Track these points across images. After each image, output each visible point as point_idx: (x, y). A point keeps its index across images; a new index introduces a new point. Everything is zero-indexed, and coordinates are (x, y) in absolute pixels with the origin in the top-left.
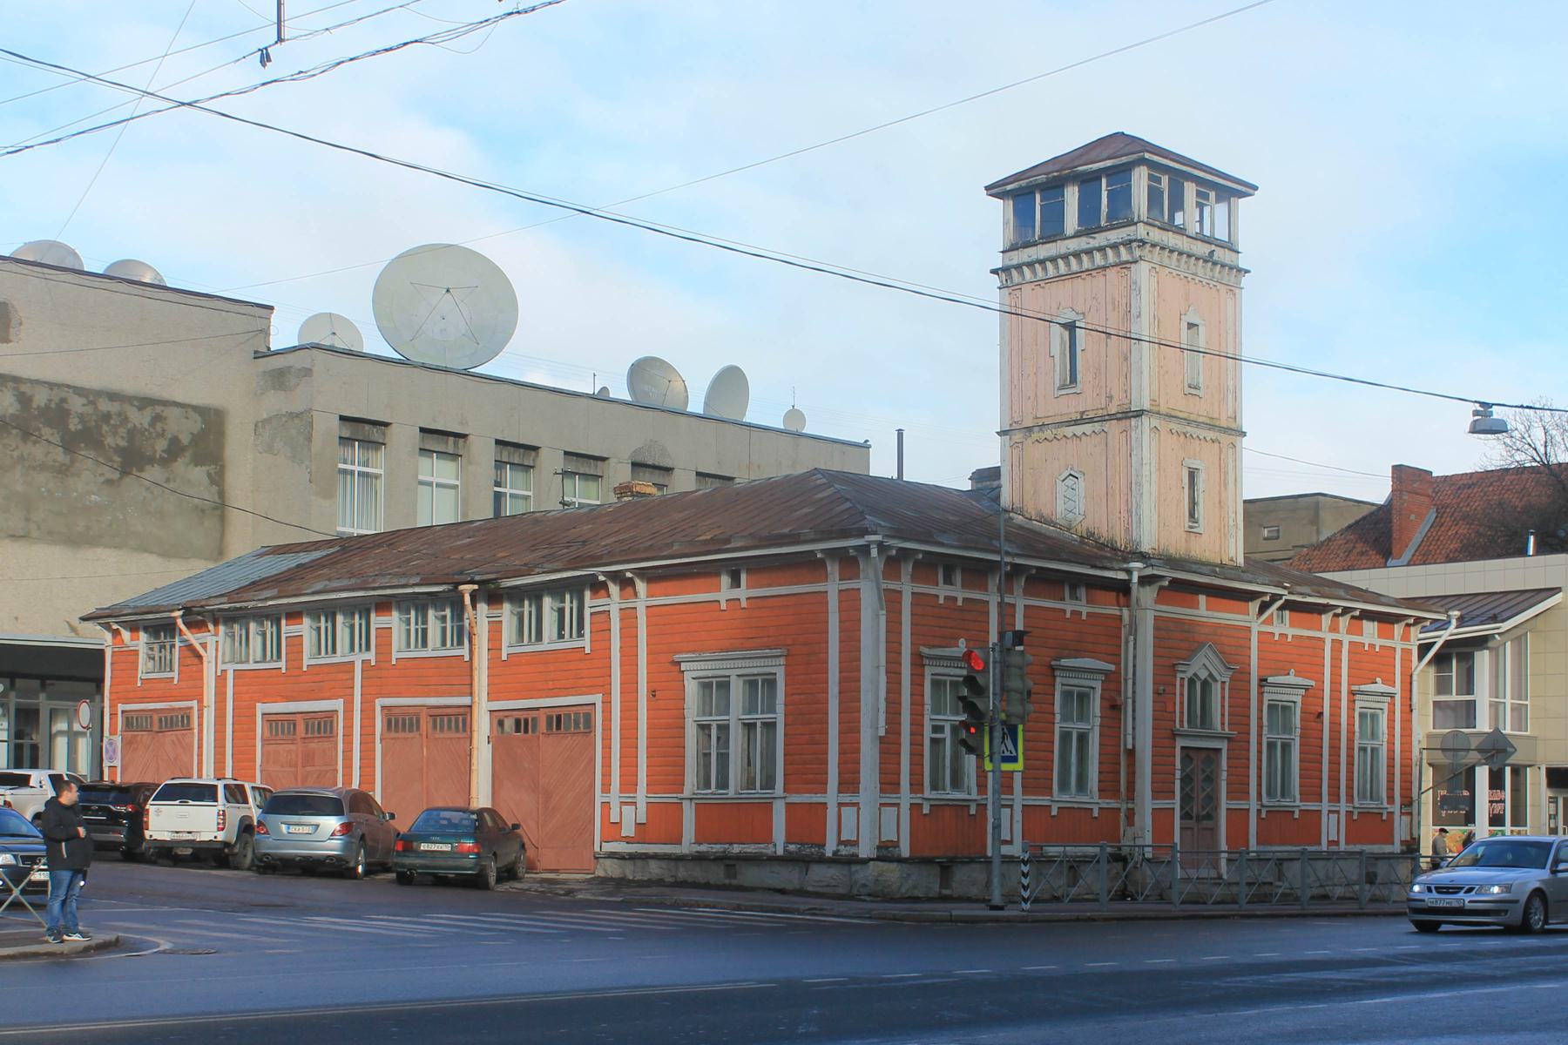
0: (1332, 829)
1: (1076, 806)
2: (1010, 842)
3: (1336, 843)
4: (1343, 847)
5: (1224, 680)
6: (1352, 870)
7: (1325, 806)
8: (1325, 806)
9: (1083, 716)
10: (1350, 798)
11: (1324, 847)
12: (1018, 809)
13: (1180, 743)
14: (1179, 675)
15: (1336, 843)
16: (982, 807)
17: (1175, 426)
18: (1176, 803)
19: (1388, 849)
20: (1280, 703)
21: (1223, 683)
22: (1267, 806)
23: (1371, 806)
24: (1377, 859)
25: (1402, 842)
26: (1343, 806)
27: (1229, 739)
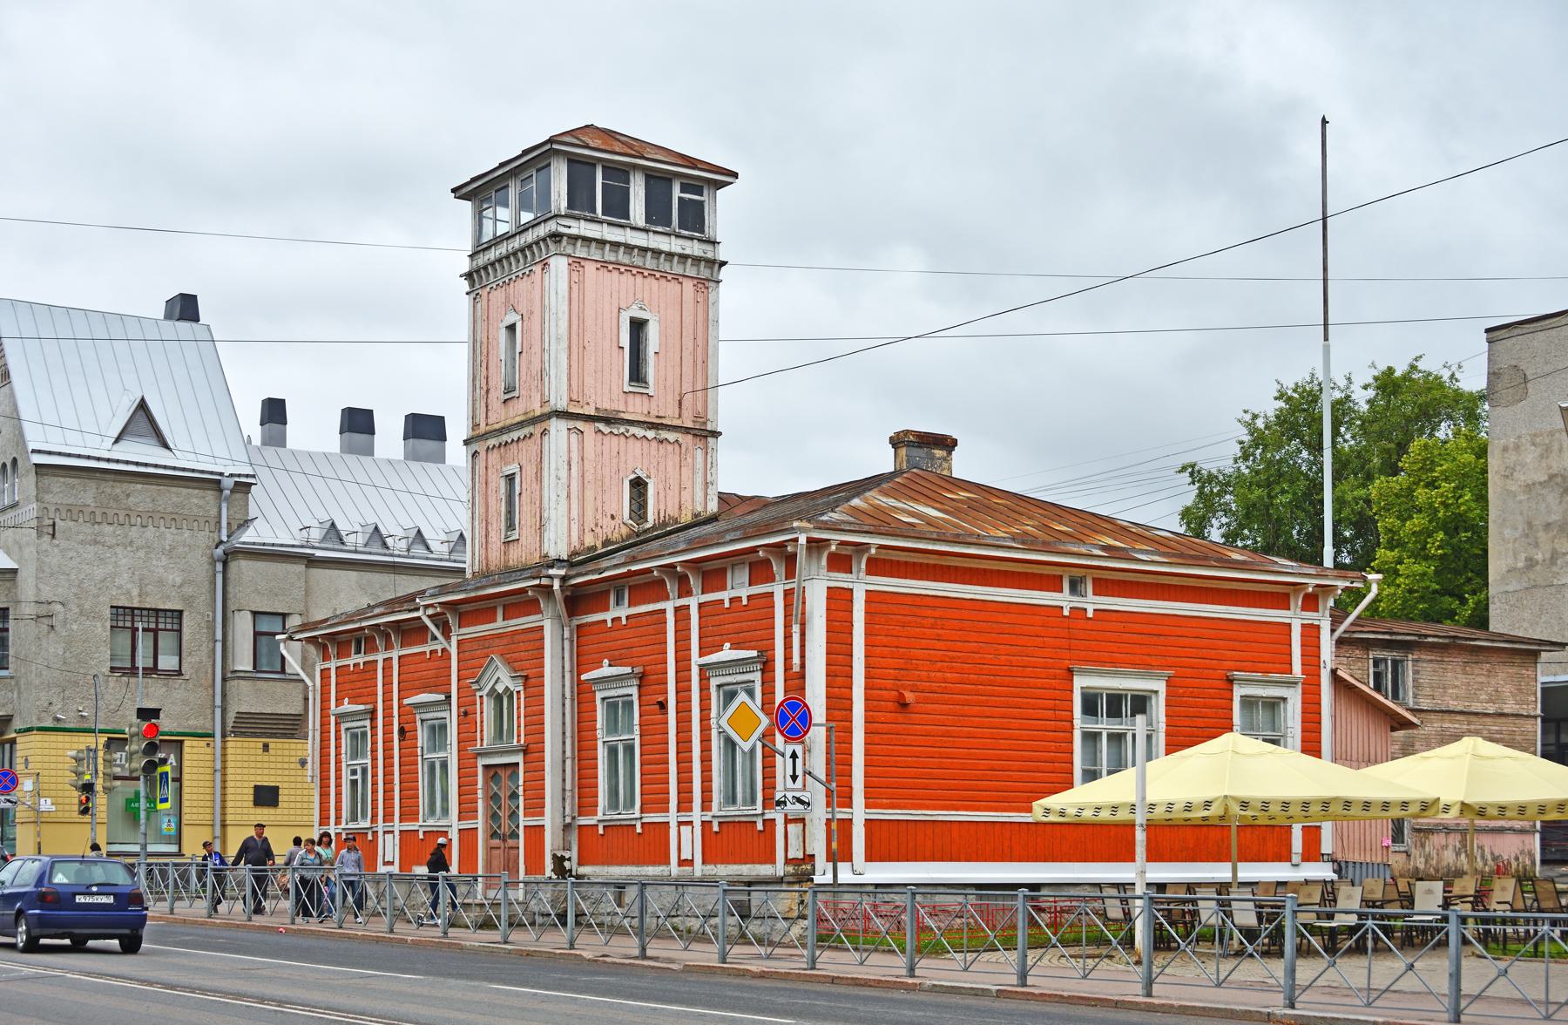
0: (687, 842)
1: (435, 829)
2: (391, 863)
3: (690, 862)
4: (699, 869)
5: (517, 689)
6: (712, 897)
7: (672, 817)
8: (672, 817)
9: (443, 747)
10: (706, 804)
11: (674, 869)
12: (397, 833)
13: (481, 762)
14: (478, 694)
15: (690, 862)
16: (375, 833)
17: (492, 442)
18: (480, 823)
19: (765, 870)
20: (620, 699)
21: (518, 692)
22: (718, 817)
23: (746, 813)
24: (749, 884)
25: (788, 861)
26: (697, 815)
27: (526, 752)
